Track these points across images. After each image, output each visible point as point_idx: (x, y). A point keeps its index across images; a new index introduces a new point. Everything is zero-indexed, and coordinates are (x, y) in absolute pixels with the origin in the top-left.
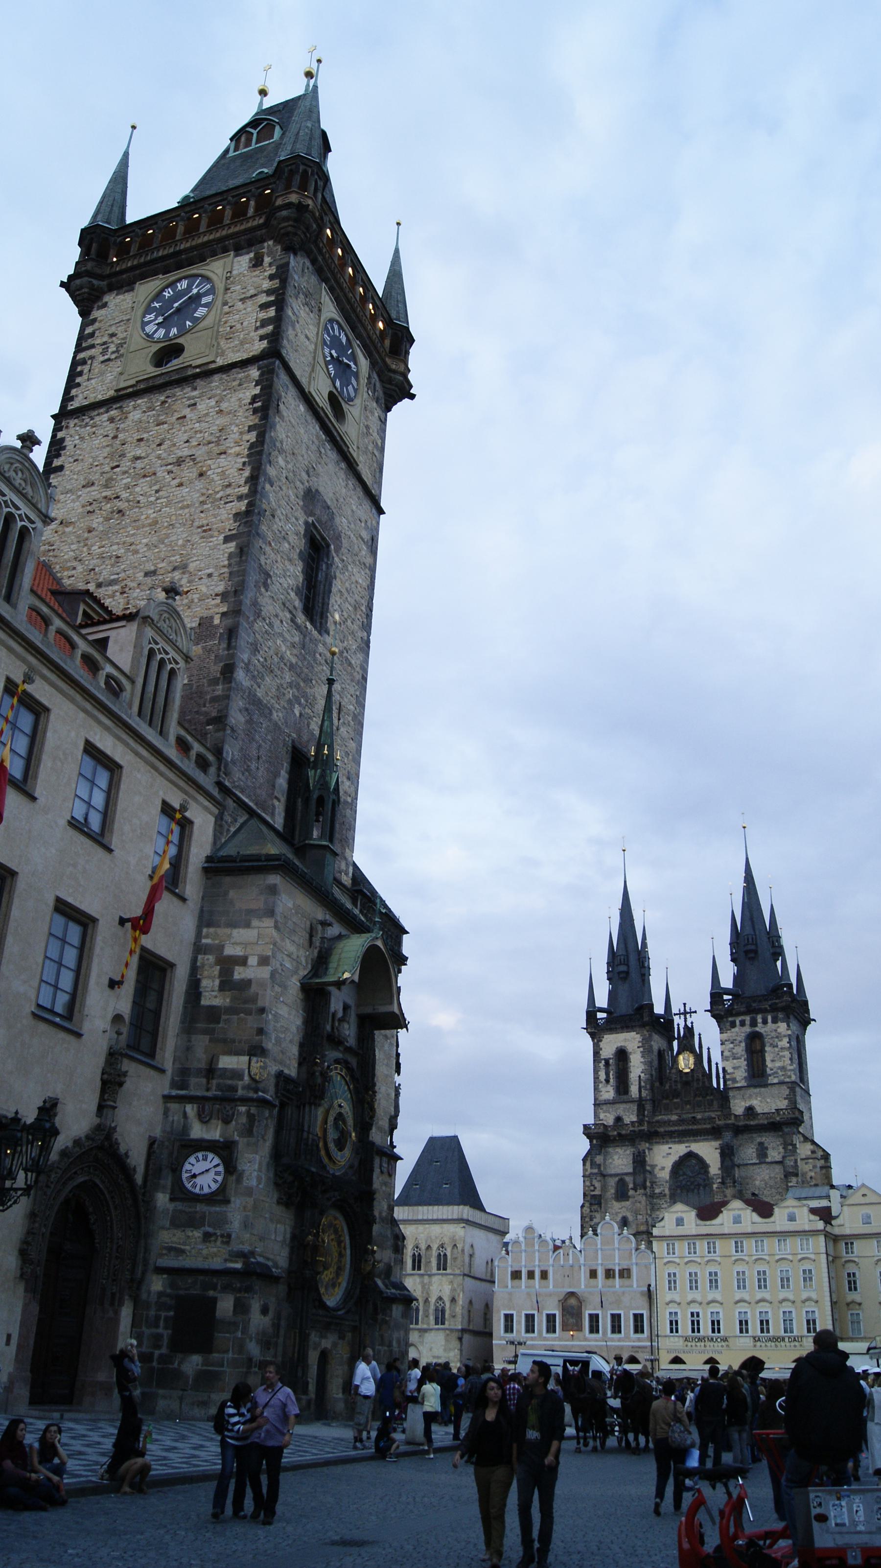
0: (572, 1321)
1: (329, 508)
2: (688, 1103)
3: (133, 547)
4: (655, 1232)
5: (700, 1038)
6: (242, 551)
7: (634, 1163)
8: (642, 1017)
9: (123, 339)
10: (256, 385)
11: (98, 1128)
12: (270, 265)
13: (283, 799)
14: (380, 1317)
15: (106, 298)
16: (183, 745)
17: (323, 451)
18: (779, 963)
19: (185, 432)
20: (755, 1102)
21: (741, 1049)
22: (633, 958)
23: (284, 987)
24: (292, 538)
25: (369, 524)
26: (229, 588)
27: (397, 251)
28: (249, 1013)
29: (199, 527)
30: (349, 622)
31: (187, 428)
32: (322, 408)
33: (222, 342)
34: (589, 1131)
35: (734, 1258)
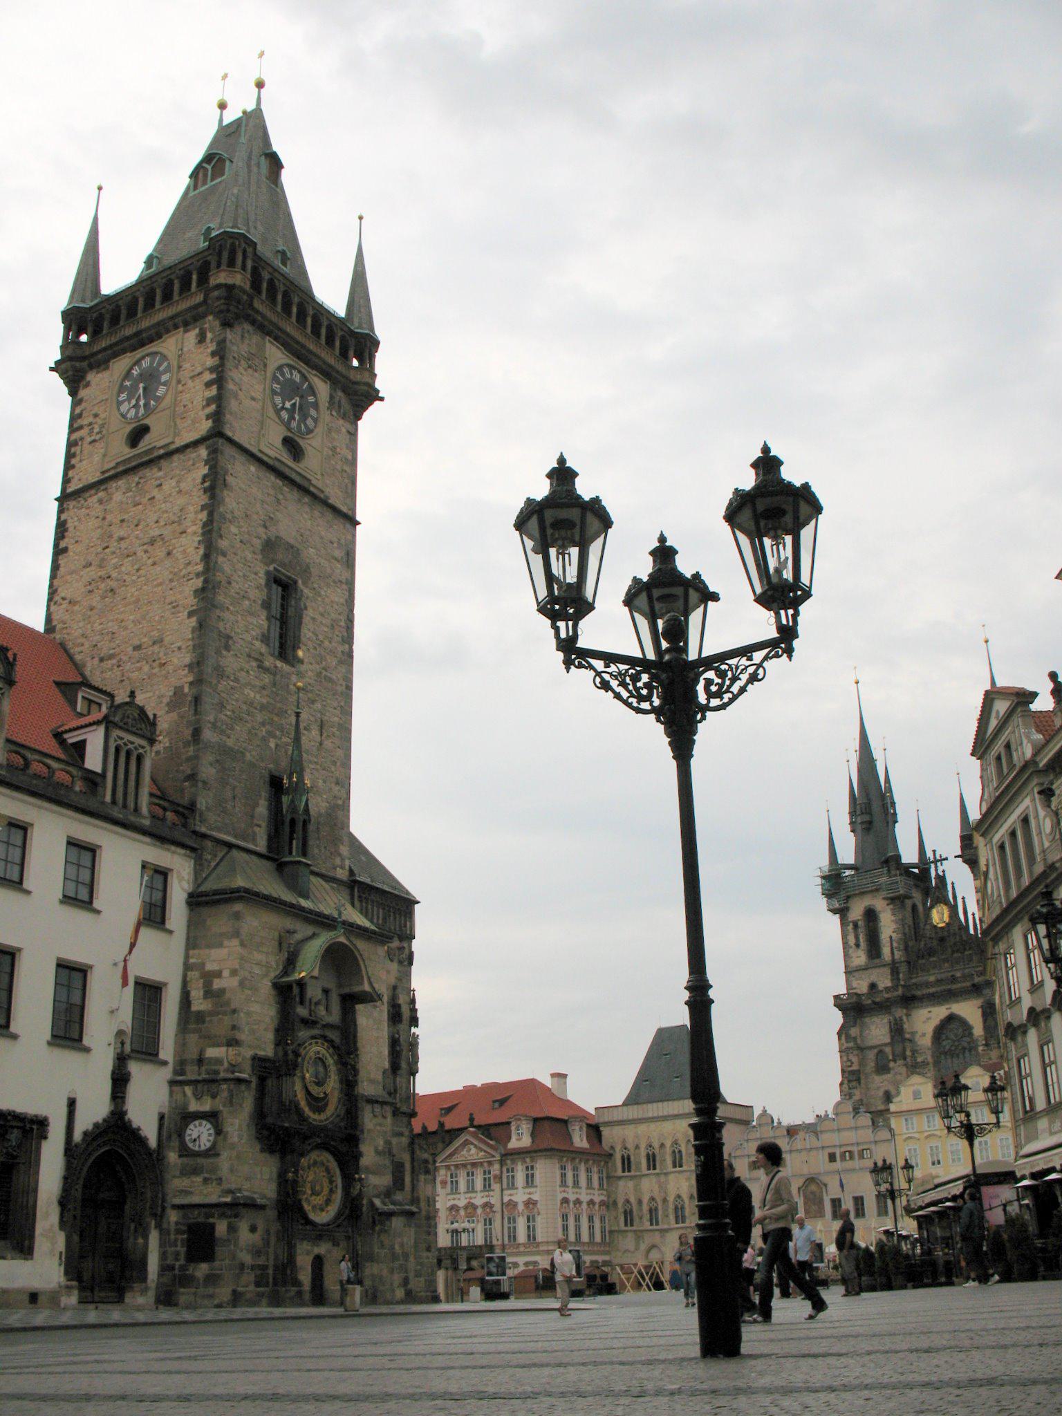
0: (814, 1208)
2: (946, 960)
4: (893, 1107)
6: (201, 625)
7: (891, 1031)
11: (113, 1113)
13: (264, 824)
14: (377, 1228)
15: (91, 377)
17: (281, 497)
22: (876, 807)
25: (343, 541)
28: (225, 1013)
30: (327, 643)
32: (276, 459)
33: (178, 421)
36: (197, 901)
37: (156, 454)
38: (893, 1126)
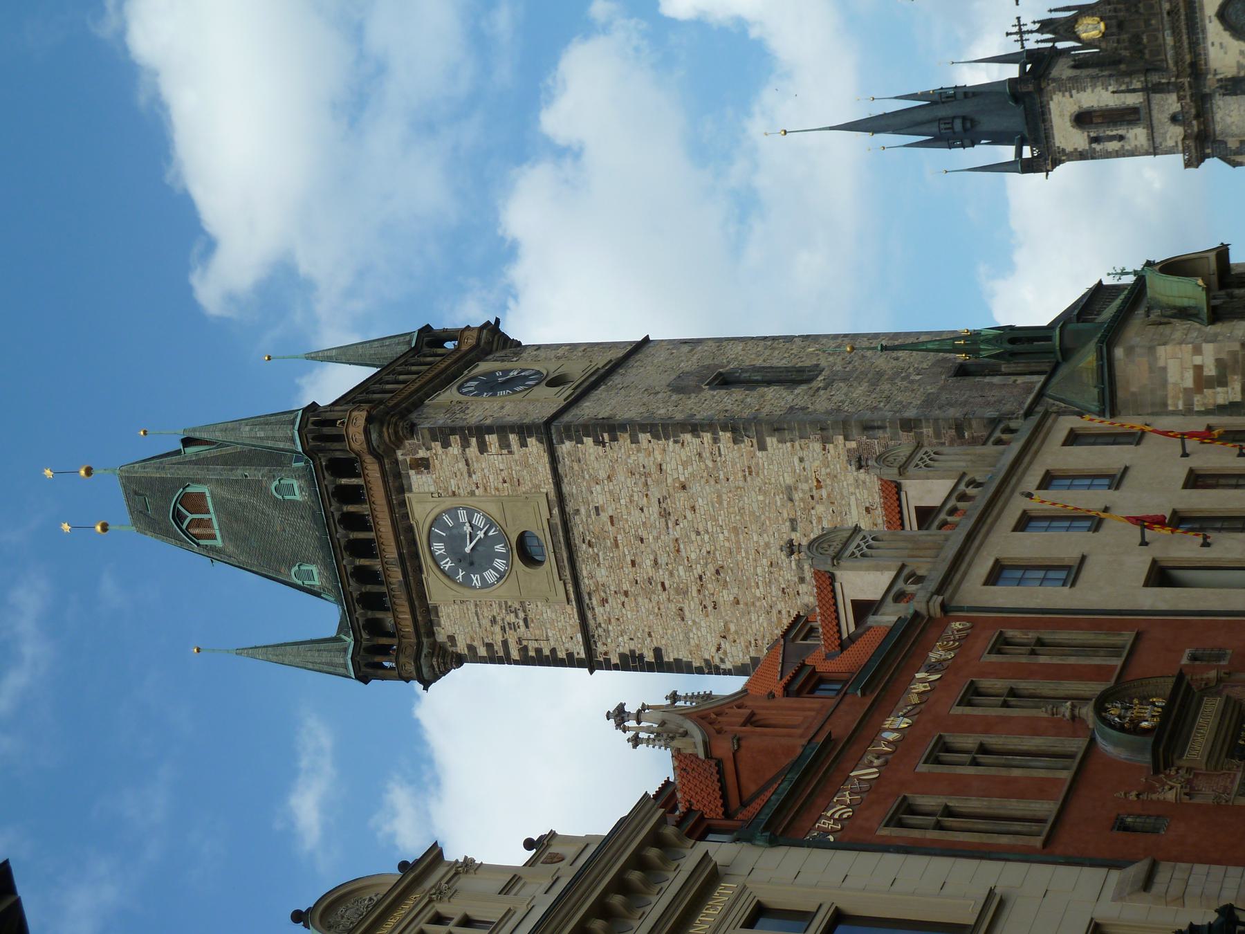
2: (1147, 22)
3: (761, 550)
5: (1056, 10)
7: (1236, 94)
8: (1029, 93)
10: (582, 443)
12: (428, 449)
15: (441, 637)
16: (999, 442)
19: (629, 514)
23: (1216, 335)
31: (625, 512)
33: (523, 489)
34: (1194, 159)
37: (557, 520)
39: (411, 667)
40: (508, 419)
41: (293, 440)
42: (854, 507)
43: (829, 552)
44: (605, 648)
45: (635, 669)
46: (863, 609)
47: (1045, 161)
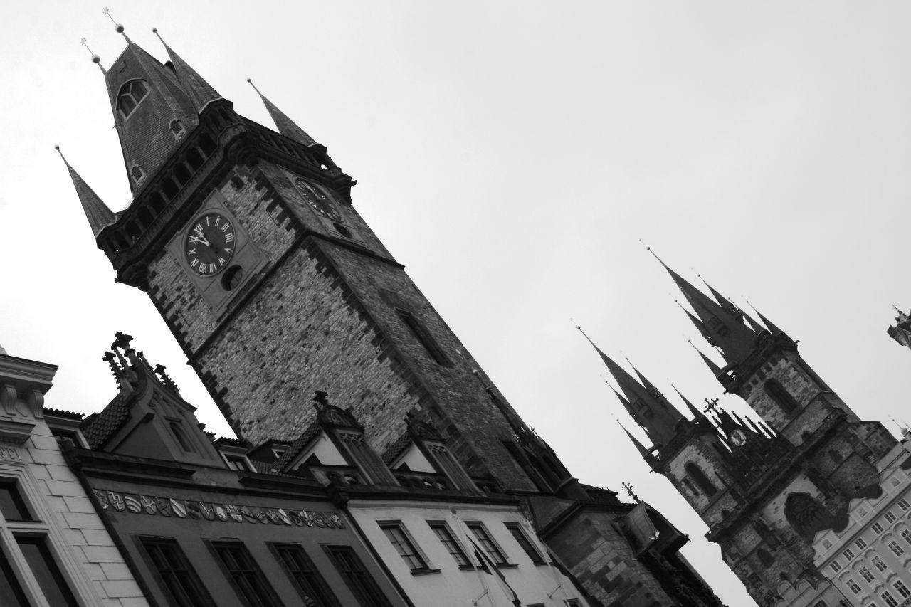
1: (391, 293)
7: (758, 533)
9: (190, 286)
10: (312, 259)
12: (249, 180)
15: (151, 269)
17: (362, 263)
18: (746, 322)
20: (805, 427)
21: (767, 400)
22: (646, 398)
23: (635, 566)
24: (402, 328)
26: (409, 385)
27: (265, 100)
29: (356, 364)
31: (289, 313)
35: (880, 539)
36: (544, 535)
37: (259, 280)
38: (826, 575)
39: (122, 263)
40: (297, 211)
41: (202, 105)
42: (382, 437)
43: (333, 421)
44: (206, 360)
45: (206, 386)
46: (314, 461)
47: (659, 466)
